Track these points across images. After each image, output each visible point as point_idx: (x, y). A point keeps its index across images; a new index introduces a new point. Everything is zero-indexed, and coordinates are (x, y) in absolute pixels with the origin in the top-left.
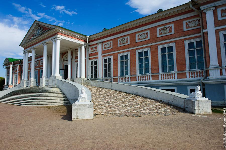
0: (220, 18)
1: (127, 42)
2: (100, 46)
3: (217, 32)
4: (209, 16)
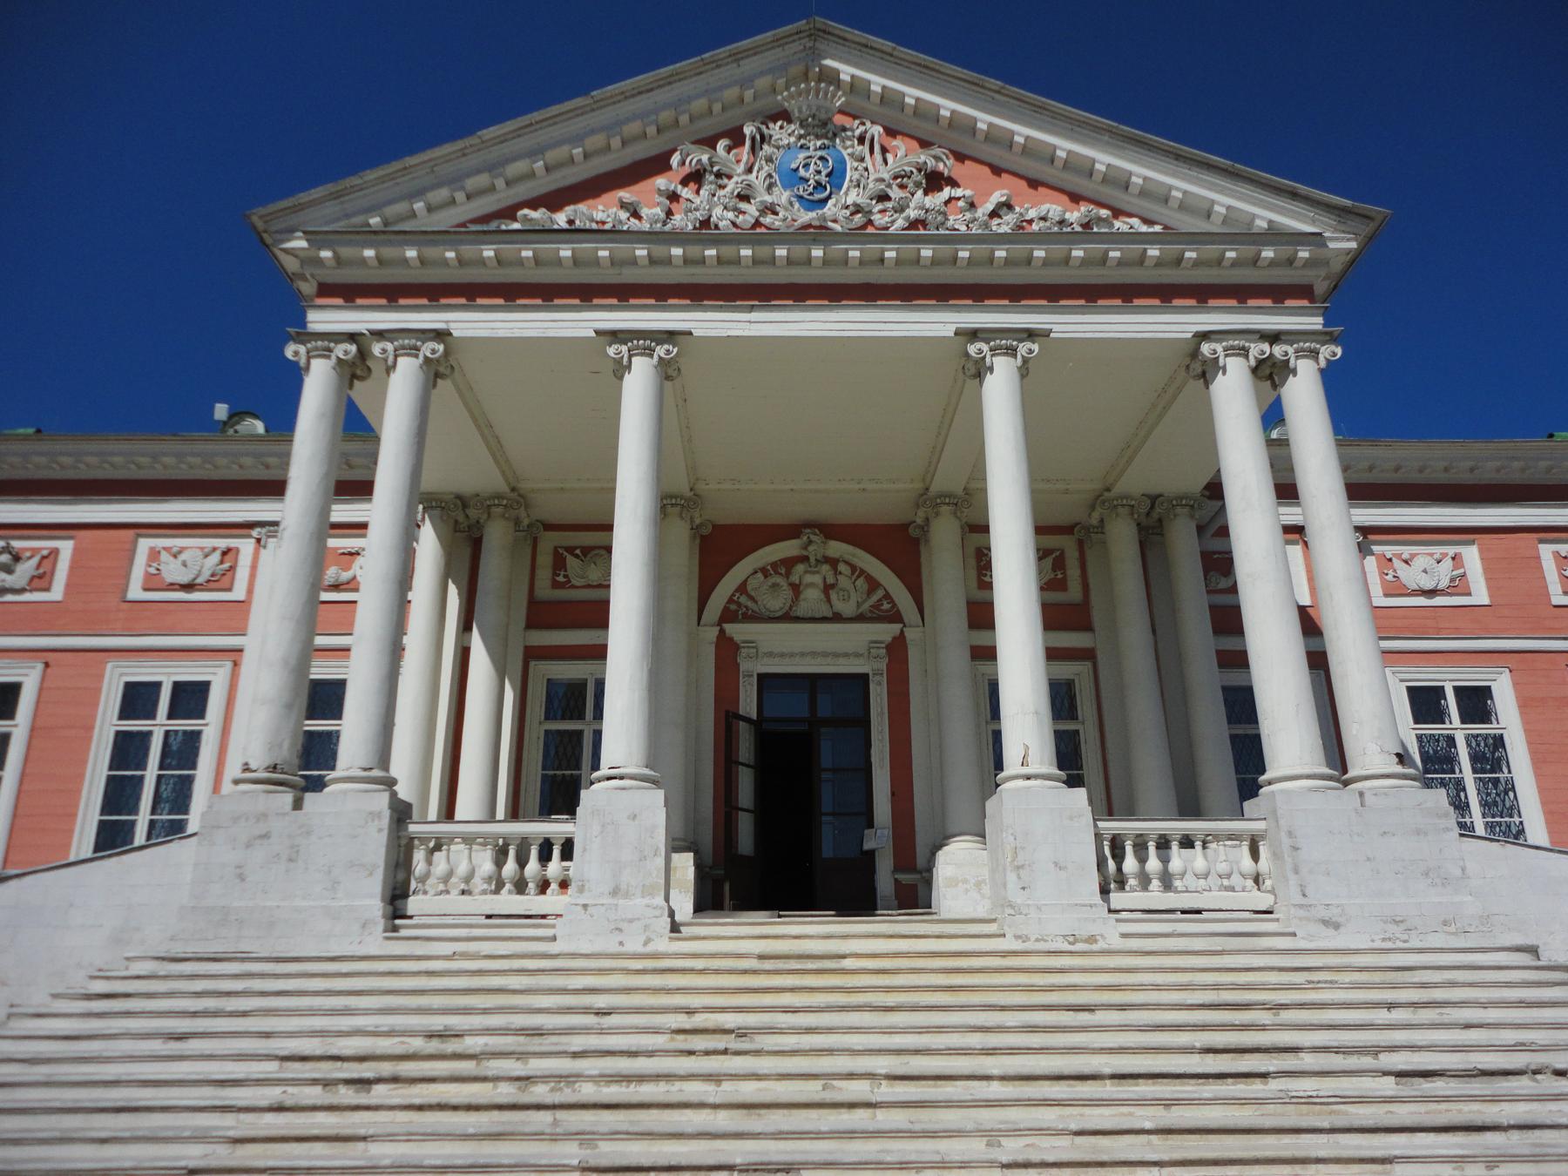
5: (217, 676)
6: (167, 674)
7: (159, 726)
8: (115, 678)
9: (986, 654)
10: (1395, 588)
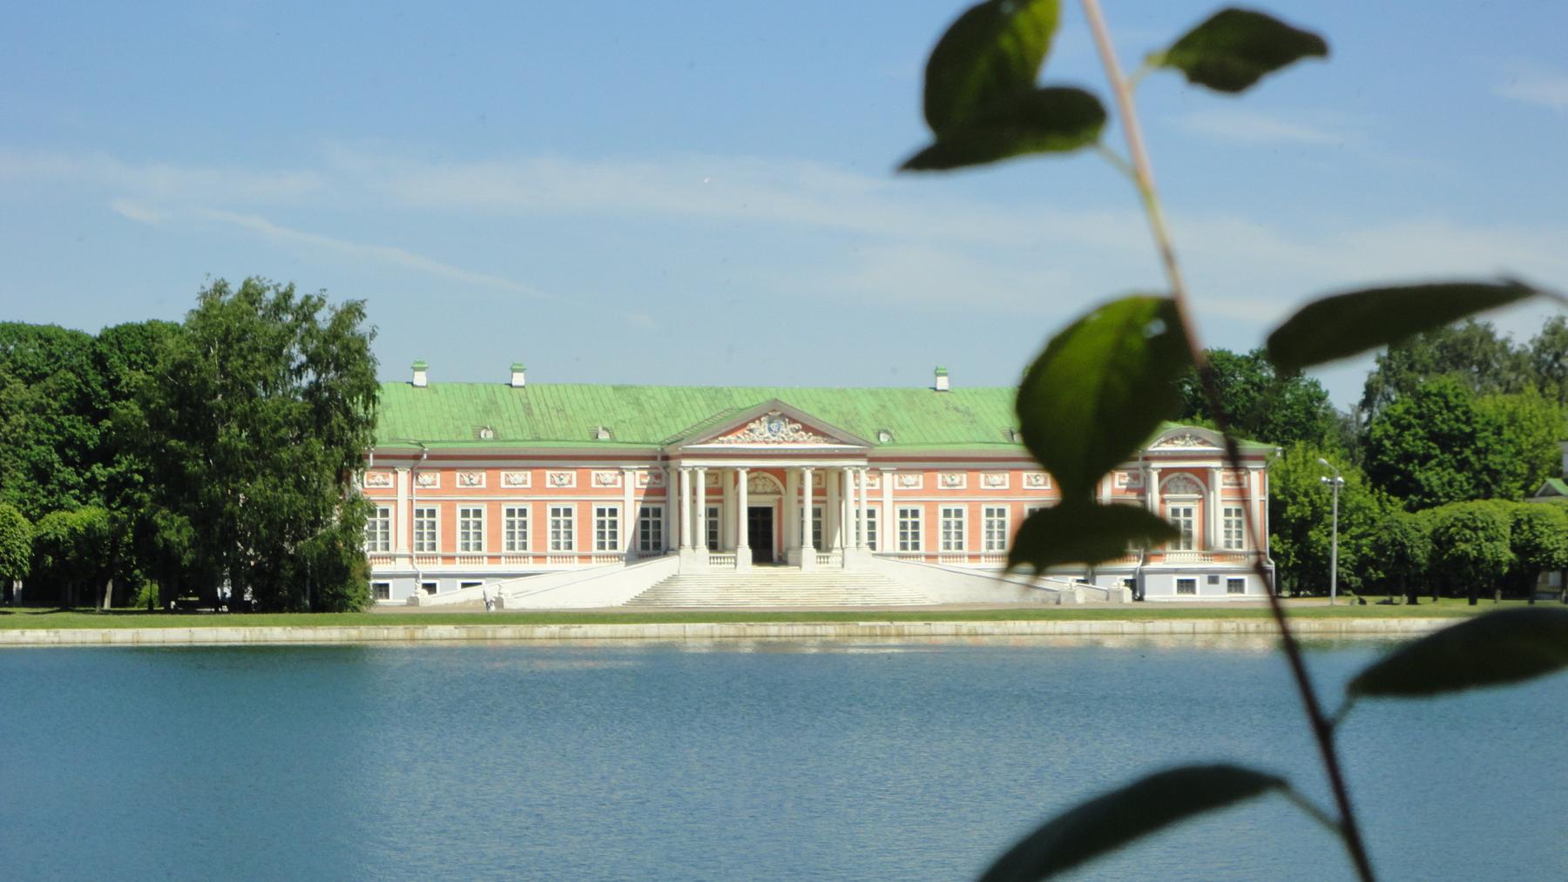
5: (619, 507)
9: (801, 502)
10: (901, 484)
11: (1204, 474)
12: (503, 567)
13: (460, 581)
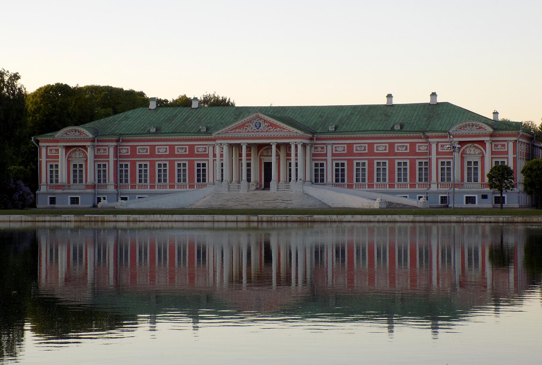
0: (440, 150)
1: (365, 150)
2: (329, 147)
3: (437, 159)
4: (434, 147)
5: (206, 162)
6: (201, 162)
7: (201, 168)
8: (196, 163)
11: (482, 143)
12: (156, 190)
13: (137, 196)
